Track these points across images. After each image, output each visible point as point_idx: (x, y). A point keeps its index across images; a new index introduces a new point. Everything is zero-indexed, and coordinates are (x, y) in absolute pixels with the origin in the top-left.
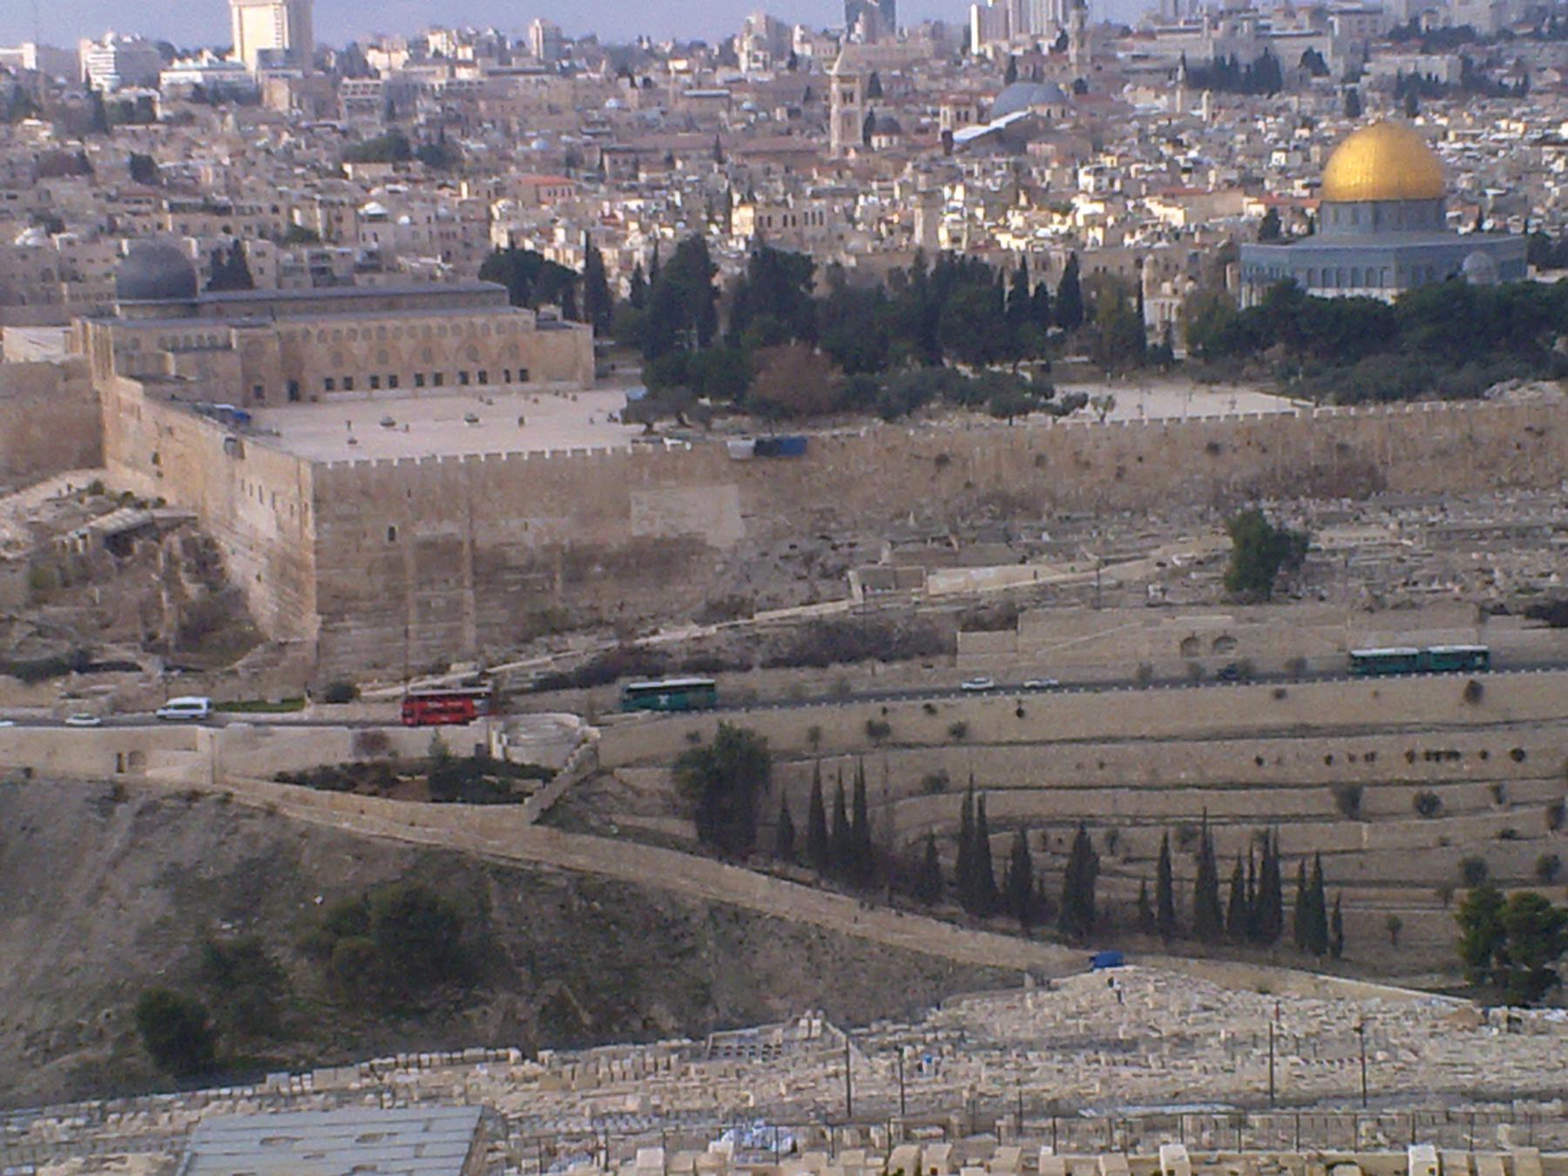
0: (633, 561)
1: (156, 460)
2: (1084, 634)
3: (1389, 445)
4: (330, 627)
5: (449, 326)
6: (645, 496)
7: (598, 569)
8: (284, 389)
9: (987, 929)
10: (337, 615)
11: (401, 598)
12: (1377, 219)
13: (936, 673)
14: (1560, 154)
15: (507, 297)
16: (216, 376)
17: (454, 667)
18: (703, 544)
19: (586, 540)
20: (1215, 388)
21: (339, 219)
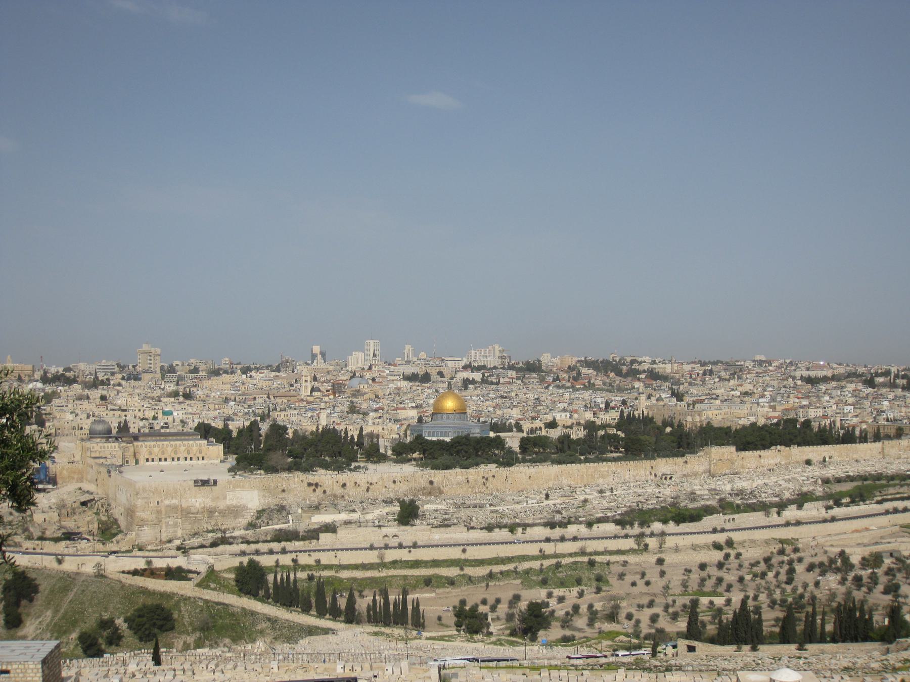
1: (97, 480)
6: (231, 493)
7: (217, 514)
10: (143, 526)
11: (160, 521)
13: (313, 544)
18: (247, 507)
19: (214, 505)
21: (157, 413)
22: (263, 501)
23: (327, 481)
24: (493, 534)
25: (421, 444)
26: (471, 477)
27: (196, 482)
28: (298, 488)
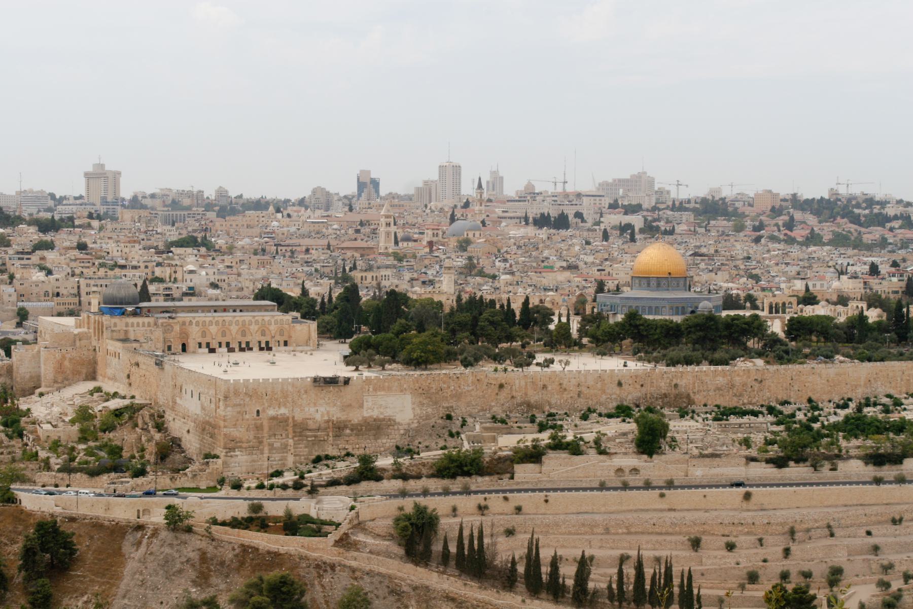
0: (364, 428)
1: (128, 377)
2: (571, 466)
3: (696, 385)
4: (229, 454)
5: (253, 320)
6: (370, 399)
7: (348, 431)
8: (181, 347)
9: (538, 598)
10: (232, 449)
11: (261, 442)
12: (659, 285)
13: (505, 483)
14: (702, 260)
16: (152, 340)
17: (285, 474)
18: (394, 421)
19: (343, 418)
20: (604, 357)
21: (175, 272)
22: (418, 411)
23: (517, 382)
24: (787, 469)
25: (637, 326)
26: (737, 379)
27: (316, 380)
28: (473, 393)
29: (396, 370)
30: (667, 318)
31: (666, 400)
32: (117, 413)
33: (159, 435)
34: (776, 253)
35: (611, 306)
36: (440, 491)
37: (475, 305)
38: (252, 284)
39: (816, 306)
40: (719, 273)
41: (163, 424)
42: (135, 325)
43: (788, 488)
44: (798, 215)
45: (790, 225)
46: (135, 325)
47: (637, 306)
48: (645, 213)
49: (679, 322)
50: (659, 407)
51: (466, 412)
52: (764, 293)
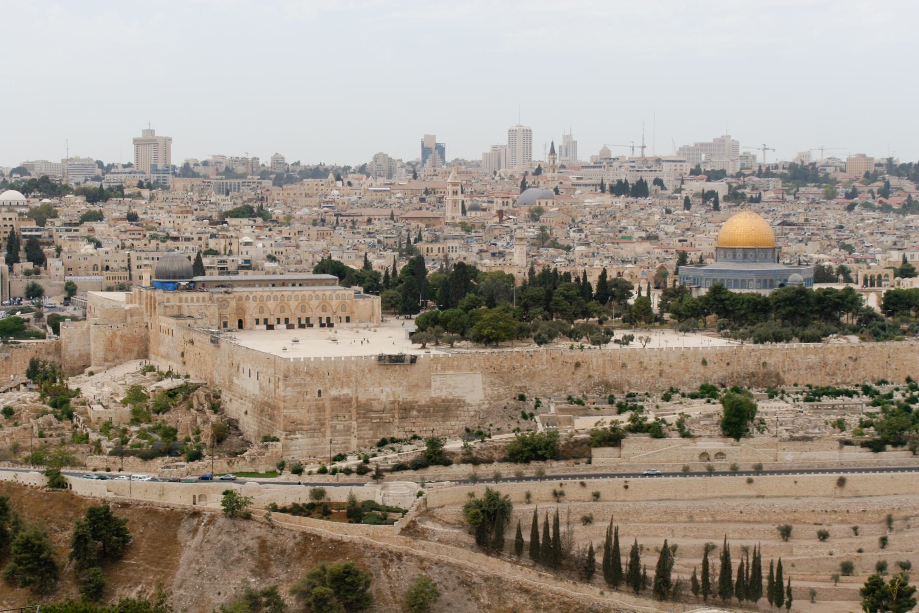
1: (183, 355)
2: (653, 449)
3: (786, 363)
4: (289, 437)
5: (313, 295)
6: (438, 378)
7: (415, 413)
8: (237, 323)
9: (617, 590)
10: (293, 432)
11: (323, 424)
12: (745, 257)
13: (582, 468)
14: (791, 229)
15: (338, 282)
16: (206, 317)
17: (349, 458)
18: (464, 402)
19: (410, 399)
20: (687, 334)
21: (230, 244)
22: (489, 391)
23: (595, 360)
24: (884, 454)
25: (722, 301)
27: (381, 358)
29: (465, 348)
30: (755, 291)
31: (754, 379)
32: (171, 393)
33: (216, 416)
34: (871, 222)
35: (695, 279)
36: (513, 476)
37: (549, 279)
38: (311, 257)
39: (914, 279)
40: (810, 243)
41: (219, 404)
42: (189, 300)
43: (885, 474)
44: (894, 181)
45: (885, 192)
46: (189, 300)
47: (722, 280)
48: (729, 180)
49: (767, 296)
50: (746, 387)
51: (541, 392)
52: (858, 265)
